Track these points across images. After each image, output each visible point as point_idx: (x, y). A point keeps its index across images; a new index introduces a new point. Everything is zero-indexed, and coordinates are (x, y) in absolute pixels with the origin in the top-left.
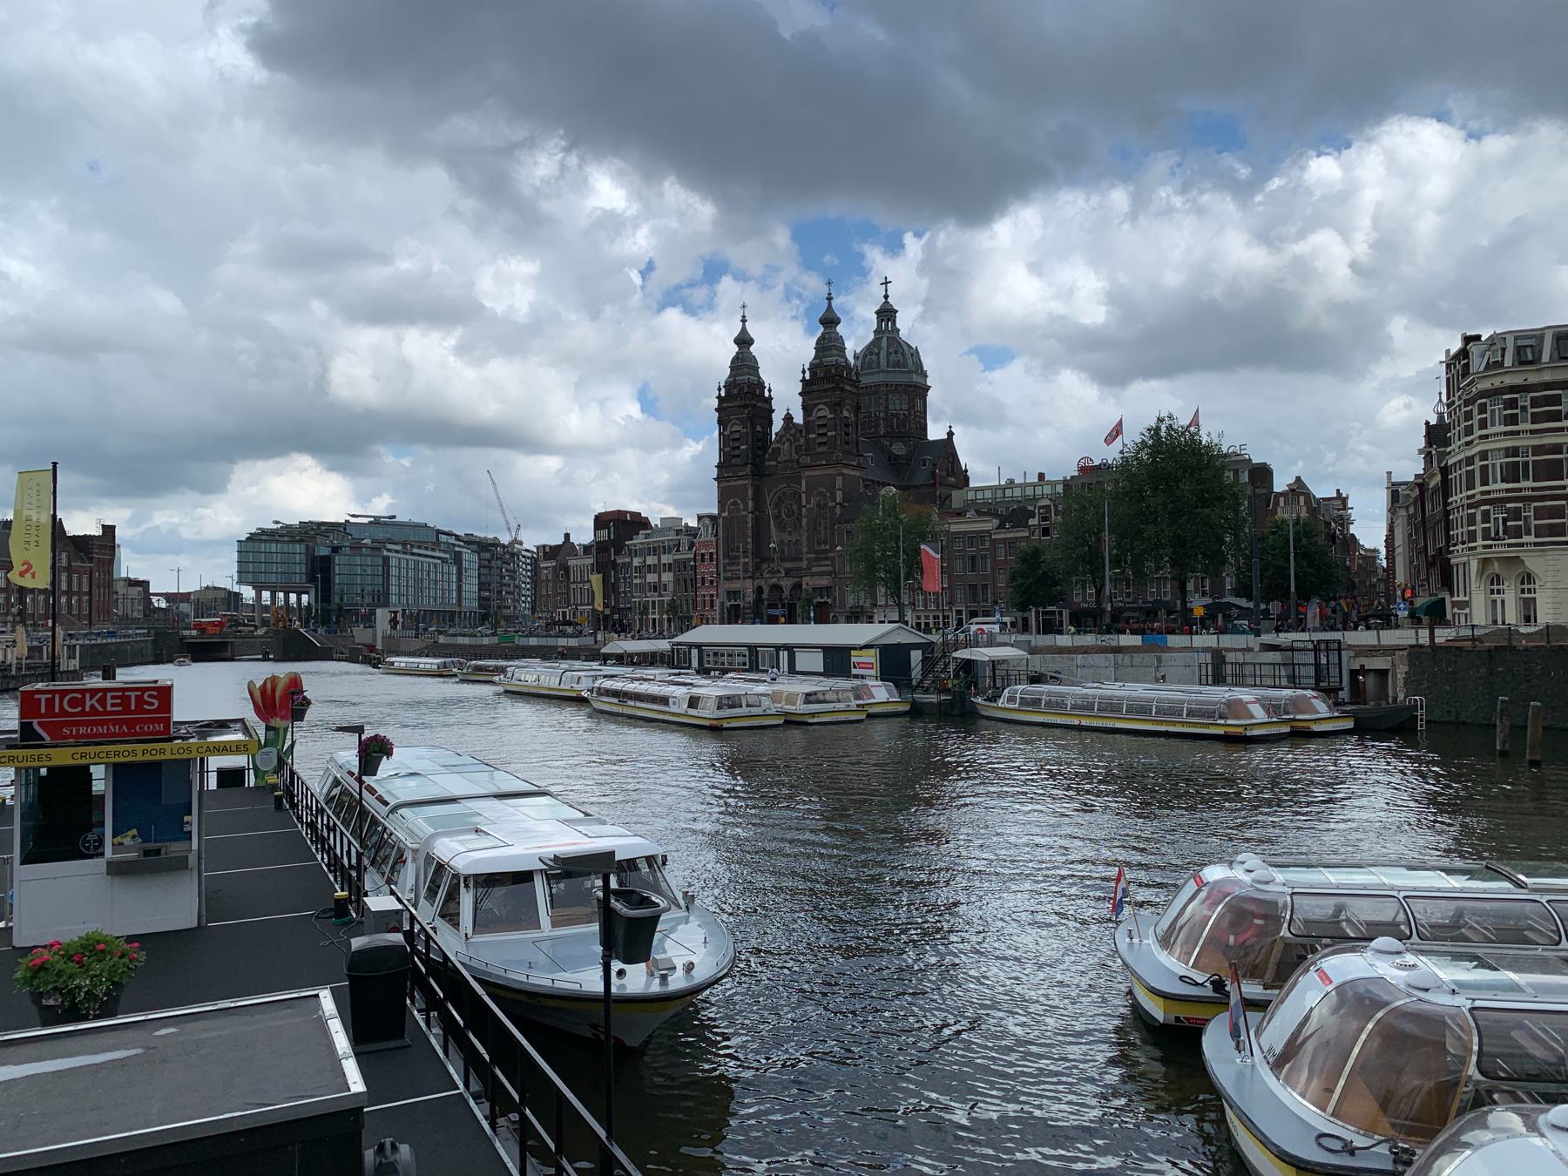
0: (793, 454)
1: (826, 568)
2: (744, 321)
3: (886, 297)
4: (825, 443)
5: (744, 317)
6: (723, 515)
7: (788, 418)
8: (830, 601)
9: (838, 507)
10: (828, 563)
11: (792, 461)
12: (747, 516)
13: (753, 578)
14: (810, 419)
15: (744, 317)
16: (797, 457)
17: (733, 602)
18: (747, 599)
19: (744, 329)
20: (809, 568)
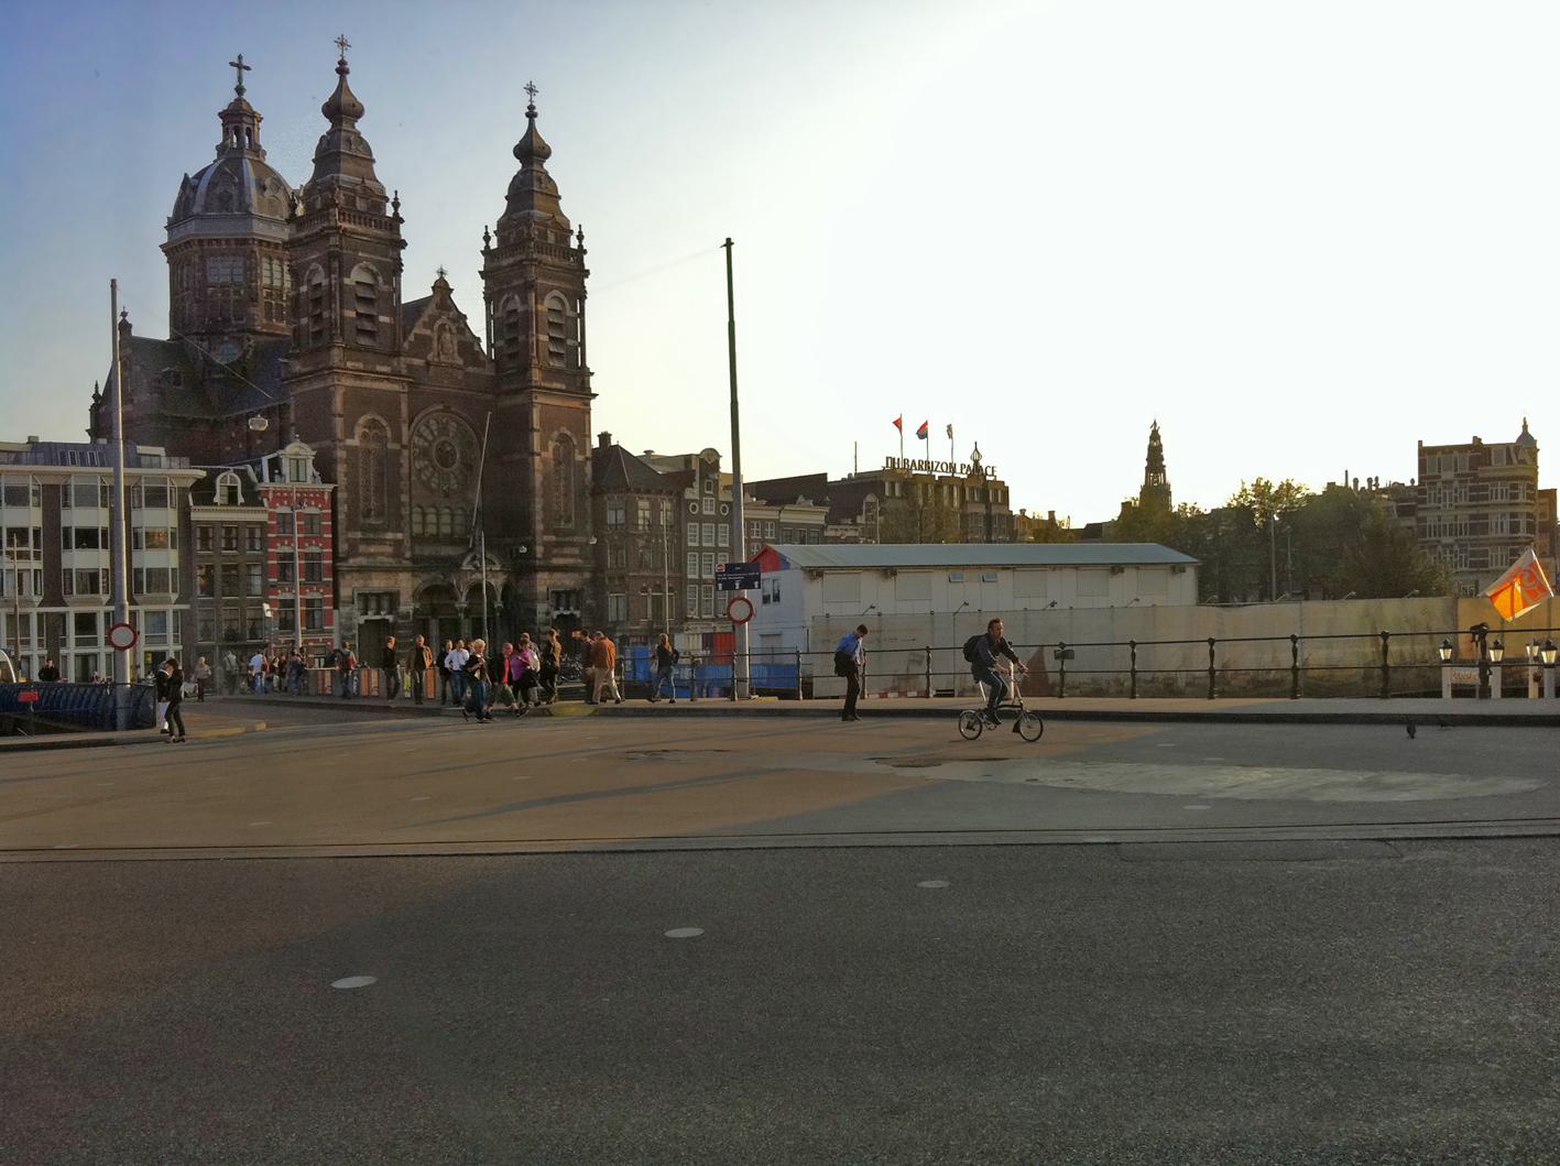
0: (456, 354)
1: (571, 561)
2: (342, 70)
3: (240, 90)
4: (558, 355)
5: (342, 62)
6: (349, 442)
7: (442, 288)
8: (577, 613)
9: (589, 464)
10: (576, 551)
11: (460, 368)
12: (398, 454)
13: (413, 571)
14: (540, 307)
15: (342, 62)
16: (460, 362)
17: (371, 616)
18: (402, 609)
19: (342, 87)
20: (547, 554)
